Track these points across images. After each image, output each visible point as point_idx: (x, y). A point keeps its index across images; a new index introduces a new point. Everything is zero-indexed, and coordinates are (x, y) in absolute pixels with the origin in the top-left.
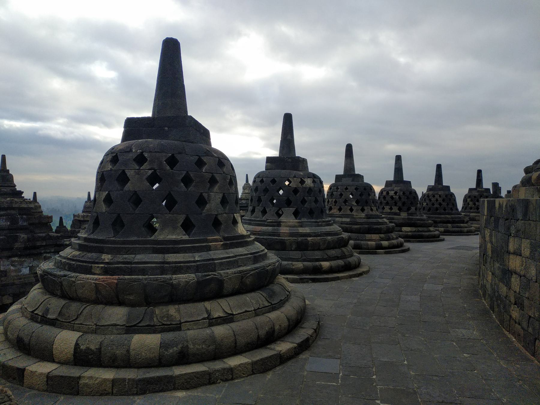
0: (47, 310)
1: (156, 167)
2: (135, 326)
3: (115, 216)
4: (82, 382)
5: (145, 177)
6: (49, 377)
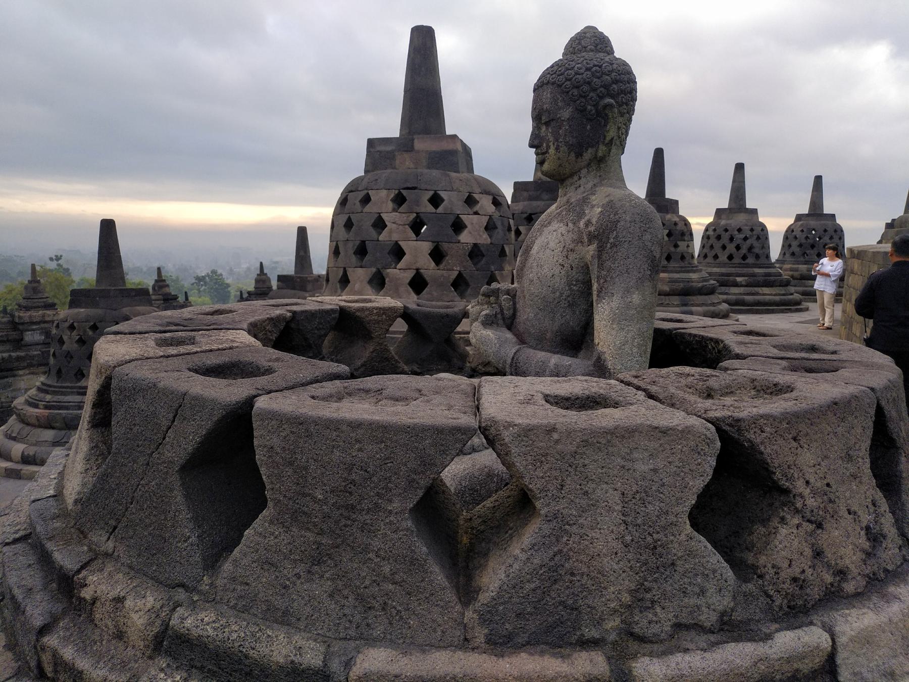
0: (12, 431)
1: (81, 334)
2: (58, 442)
4: (22, 472)
6: (6, 469)
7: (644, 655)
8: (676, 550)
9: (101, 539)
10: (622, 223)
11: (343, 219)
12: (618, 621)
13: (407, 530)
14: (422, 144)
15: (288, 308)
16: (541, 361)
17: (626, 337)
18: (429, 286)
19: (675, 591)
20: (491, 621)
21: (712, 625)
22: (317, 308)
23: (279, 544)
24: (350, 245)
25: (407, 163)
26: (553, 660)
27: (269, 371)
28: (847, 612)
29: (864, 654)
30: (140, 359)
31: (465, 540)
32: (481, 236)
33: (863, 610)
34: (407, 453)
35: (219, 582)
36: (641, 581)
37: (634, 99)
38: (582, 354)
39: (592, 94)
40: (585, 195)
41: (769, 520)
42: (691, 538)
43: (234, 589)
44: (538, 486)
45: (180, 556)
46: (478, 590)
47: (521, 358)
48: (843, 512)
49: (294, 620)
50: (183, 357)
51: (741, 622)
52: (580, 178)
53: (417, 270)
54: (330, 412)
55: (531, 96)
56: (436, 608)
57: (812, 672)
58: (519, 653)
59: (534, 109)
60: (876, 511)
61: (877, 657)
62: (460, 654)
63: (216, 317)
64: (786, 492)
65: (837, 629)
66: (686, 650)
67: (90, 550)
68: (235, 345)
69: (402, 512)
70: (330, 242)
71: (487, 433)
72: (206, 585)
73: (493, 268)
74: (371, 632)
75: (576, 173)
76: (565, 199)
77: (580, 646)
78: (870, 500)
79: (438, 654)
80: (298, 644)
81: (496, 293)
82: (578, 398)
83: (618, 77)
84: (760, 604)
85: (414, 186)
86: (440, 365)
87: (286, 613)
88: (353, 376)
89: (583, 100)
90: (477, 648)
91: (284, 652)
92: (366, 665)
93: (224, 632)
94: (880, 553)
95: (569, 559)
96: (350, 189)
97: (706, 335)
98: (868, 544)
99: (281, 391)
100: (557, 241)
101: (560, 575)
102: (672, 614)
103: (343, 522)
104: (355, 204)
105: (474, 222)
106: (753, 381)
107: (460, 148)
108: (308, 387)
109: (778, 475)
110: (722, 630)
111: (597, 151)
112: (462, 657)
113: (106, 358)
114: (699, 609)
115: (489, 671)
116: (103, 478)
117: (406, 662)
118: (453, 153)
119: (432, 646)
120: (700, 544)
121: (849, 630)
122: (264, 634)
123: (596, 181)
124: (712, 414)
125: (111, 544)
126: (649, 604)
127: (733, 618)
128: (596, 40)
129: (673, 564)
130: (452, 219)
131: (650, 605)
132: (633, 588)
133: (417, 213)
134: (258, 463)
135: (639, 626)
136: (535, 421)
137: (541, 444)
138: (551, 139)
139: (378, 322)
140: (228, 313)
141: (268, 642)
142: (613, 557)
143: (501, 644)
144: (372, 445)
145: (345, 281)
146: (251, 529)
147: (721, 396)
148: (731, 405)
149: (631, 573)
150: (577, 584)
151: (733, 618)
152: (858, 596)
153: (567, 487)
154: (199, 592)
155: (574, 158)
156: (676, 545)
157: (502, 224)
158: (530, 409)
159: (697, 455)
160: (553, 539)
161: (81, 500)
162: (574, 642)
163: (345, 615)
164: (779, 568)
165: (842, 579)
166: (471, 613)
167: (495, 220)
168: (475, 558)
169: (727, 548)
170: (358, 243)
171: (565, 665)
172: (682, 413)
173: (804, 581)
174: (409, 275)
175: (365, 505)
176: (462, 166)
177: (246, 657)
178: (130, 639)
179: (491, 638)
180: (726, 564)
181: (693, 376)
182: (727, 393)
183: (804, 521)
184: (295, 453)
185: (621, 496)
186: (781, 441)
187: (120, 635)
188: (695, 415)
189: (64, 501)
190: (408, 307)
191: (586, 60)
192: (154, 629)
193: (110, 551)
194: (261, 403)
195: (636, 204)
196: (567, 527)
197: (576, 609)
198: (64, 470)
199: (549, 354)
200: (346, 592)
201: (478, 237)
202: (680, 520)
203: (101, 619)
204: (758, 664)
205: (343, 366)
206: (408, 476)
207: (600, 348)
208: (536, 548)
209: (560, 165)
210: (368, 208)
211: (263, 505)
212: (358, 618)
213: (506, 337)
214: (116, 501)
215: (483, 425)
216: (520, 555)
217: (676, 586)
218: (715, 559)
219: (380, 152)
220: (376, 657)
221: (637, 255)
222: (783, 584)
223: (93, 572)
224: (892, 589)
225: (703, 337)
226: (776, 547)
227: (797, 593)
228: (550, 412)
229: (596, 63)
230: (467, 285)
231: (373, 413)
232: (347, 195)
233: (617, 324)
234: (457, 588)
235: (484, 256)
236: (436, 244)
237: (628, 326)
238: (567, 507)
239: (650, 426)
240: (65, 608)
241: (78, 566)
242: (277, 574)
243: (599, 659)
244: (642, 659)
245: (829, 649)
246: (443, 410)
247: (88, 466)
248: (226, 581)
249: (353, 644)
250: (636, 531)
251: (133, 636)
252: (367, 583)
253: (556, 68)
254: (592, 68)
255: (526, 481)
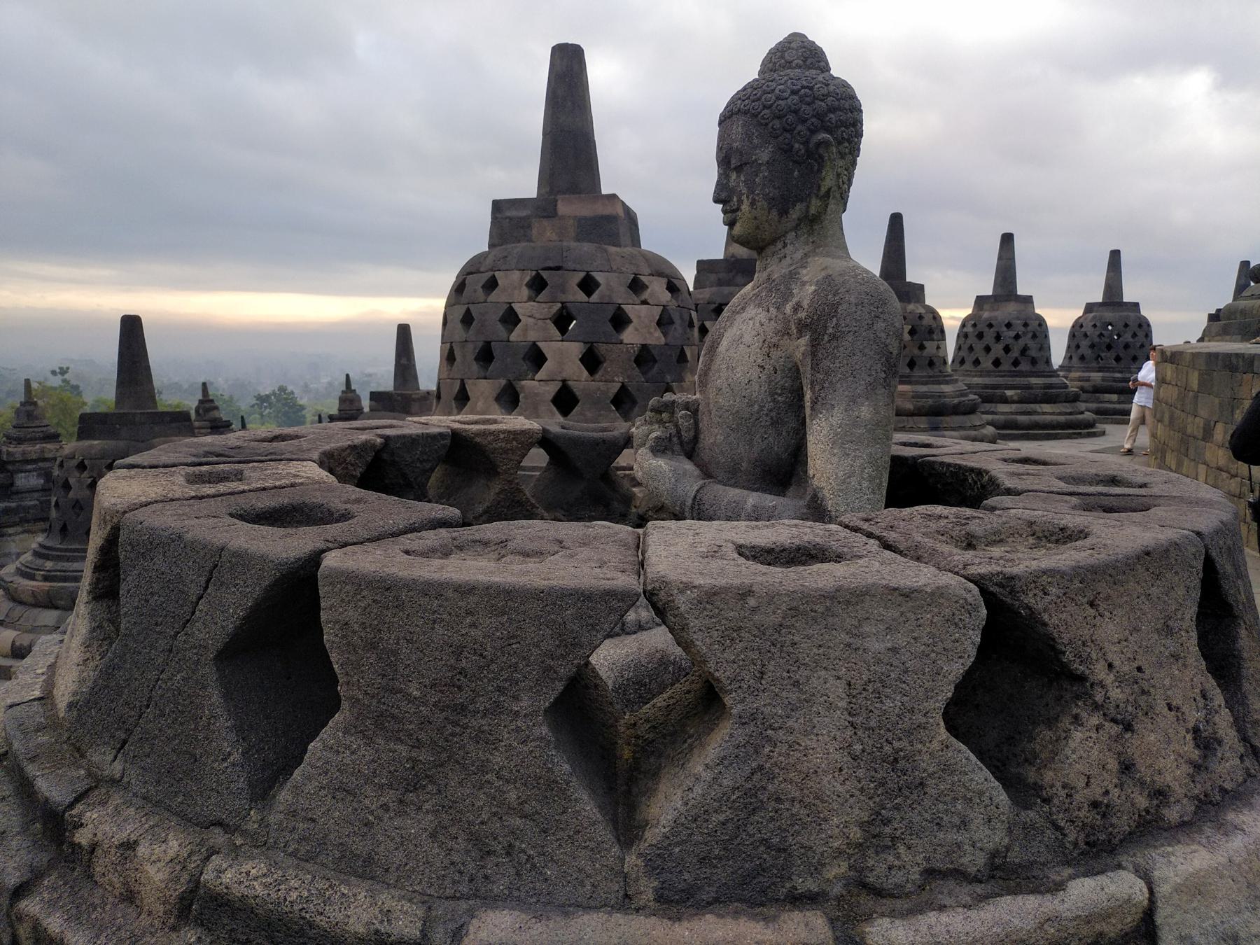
3: (61, 523)
5: (85, 486)
7: (883, 915)
8: (926, 764)
9: (104, 759)
10: (845, 306)
11: (460, 311)
12: (844, 866)
13: (542, 739)
14: (568, 208)
15: (379, 431)
16: (734, 502)
17: (852, 466)
18: (579, 404)
19: (924, 823)
20: (663, 869)
21: (978, 871)
22: (420, 431)
23: (358, 762)
24: (470, 346)
25: (548, 234)
26: (752, 924)
27: (345, 517)
28: (1170, 849)
29: (1195, 909)
30: (162, 501)
31: (627, 753)
32: (651, 333)
33: (1193, 847)
34: (540, 629)
35: (272, 819)
36: (877, 809)
37: (860, 135)
38: (792, 490)
39: (800, 127)
40: (792, 268)
41: (1057, 719)
42: (947, 747)
43: (294, 828)
44: (728, 673)
45: (217, 782)
46: (645, 825)
47: (705, 498)
48: (1161, 707)
49: (379, 871)
50: (224, 498)
51: (1020, 865)
52: (785, 245)
53: (564, 381)
54: (430, 572)
55: (716, 130)
56: (583, 851)
57: (1122, 937)
58: (703, 915)
59: (720, 149)
60: (1207, 705)
61: (1213, 914)
62: (618, 917)
63: (275, 444)
64: (1082, 679)
65: (1156, 873)
66: (942, 908)
67: (89, 774)
68: (298, 481)
69: (533, 714)
70: (442, 343)
71: (655, 599)
72: (254, 822)
73: (668, 378)
74: (490, 886)
75: (779, 238)
76: (765, 274)
77: (791, 903)
78: (1198, 691)
79: (586, 917)
80: (386, 907)
81: (670, 407)
82: (784, 550)
83: (837, 103)
84: (1046, 839)
85: (557, 265)
86: (594, 511)
87: (369, 861)
88: (466, 524)
89: (788, 135)
90: (644, 908)
91: (365, 917)
92: (483, 935)
93: (279, 890)
94: (1214, 765)
95: (773, 779)
96: (468, 270)
97: (964, 463)
98: (1196, 752)
99: (362, 543)
100: (754, 333)
101: (761, 801)
102: (922, 856)
103: (450, 728)
104: (475, 291)
105: (642, 315)
106: (1031, 524)
107: (621, 212)
108: (401, 539)
109: (1069, 656)
110: (993, 877)
111: (808, 207)
112: (621, 921)
113: (113, 501)
114: (959, 847)
115: (659, 941)
116: (108, 672)
117: (540, 930)
118: (612, 219)
119: (578, 906)
120: (960, 755)
121: (1172, 874)
122: (336, 892)
123: (807, 248)
124: (974, 570)
125: (118, 767)
126: (888, 842)
127: (1008, 860)
128: (805, 52)
129: (921, 784)
130: (610, 311)
131: (890, 844)
132: (866, 819)
133: (562, 303)
134: (327, 646)
135: (874, 873)
136: (722, 582)
137: (732, 614)
138: (745, 190)
139: (506, 451)
140: (293, 439)
141: (342, 903)
142: (836, 775)
143: (678, 902)
144: (490, 618)
145: (462, 398)
146: (318, 742)
147: (986, 546)
148: (1001, 558)
149: (862, 798)
150: (786, 814)
151: (1008, 860)
152: (1185, 827)
153: (770, 674)
154: (245, 833)
155: (776, 219)
156: (926, 757)
157: (682, 318)
158: (715, 564)
159: (953, 627)
160: (751, 751)
161: (77, 703)
162: (782, 897)
163: (452, 863)
164: (1072, 789)
165: (1161, 803)
166: (634, 857)
167: (671, 312)
168: (641, 779)
169: (998, 760)
170: (480, 344)
171: (769, 932)
172: (933, 569)
173: (1107, 806)
174: (553, 388)
175: (481, 704)
176: (625, 238)
177: (311, 925)
178: (145, 901)
179: (662, 894)
180: (997, 783)
181: (947, 518)
182: (994, 541)
183: (1106, 720)
184: (379, 631)
185: (847, 687)
186: (1071, 607)
187: (130, 897)
188: (951, 572)
189: (54, 705)
190: (548, 430)
191: (792, 79)
192: (178, 887)
193: (118, 776)
194: (332, 560)
195: (863, 279)
196: (770, 732)
197: (784, 849)
198: (56, 662)
199: (746, 492)
200: (454, 831)
201: (648, 336)
202: (931, 720)
203: (104, 874)
204: (1045, 926)
205: (451, 508)
206: (543, 662)
207: (815, 482)
208: (726, 762)
209: (757, 228)
210: (493, 297)
211: (336, 707)
212: (471, 867)
213: (685, 469)
214: (127, 704)
215: (649, 588)
216: (703, 774)
217: (926, 815)
218: (981, 777)
219: (511, 219)
220: (497, 923)
221: (866, 350)
222: (1079, 810)
223: (91, 807)
224: (1231, 816)
225: (960, 467)
226: (1067, 758)
227: (1098, 823)
228: (744, 569)
229: (804, 83)
230: (634, 402)
231: (491, 572)
232: (464, 280)
233: (839, 448)
234: (614, 822)
235: (655, 361)
236: (589, 345)
237: (855, 450)
238: (770, 704)
239: (886, 587)
240: (52, 859)
241: (71, 798)
242: (355, 804)
243: (819, 922)
244: (880, 921)
245: (1146, 902)
246: (592, 568)
247: (88, 655)
248: (282, 816)
249: (463, 905)
250: (869, 737)
251: (149, 898)
252: (485, 816)
253: (749, 90)
254: (800, 90)
255: (711, 666)
